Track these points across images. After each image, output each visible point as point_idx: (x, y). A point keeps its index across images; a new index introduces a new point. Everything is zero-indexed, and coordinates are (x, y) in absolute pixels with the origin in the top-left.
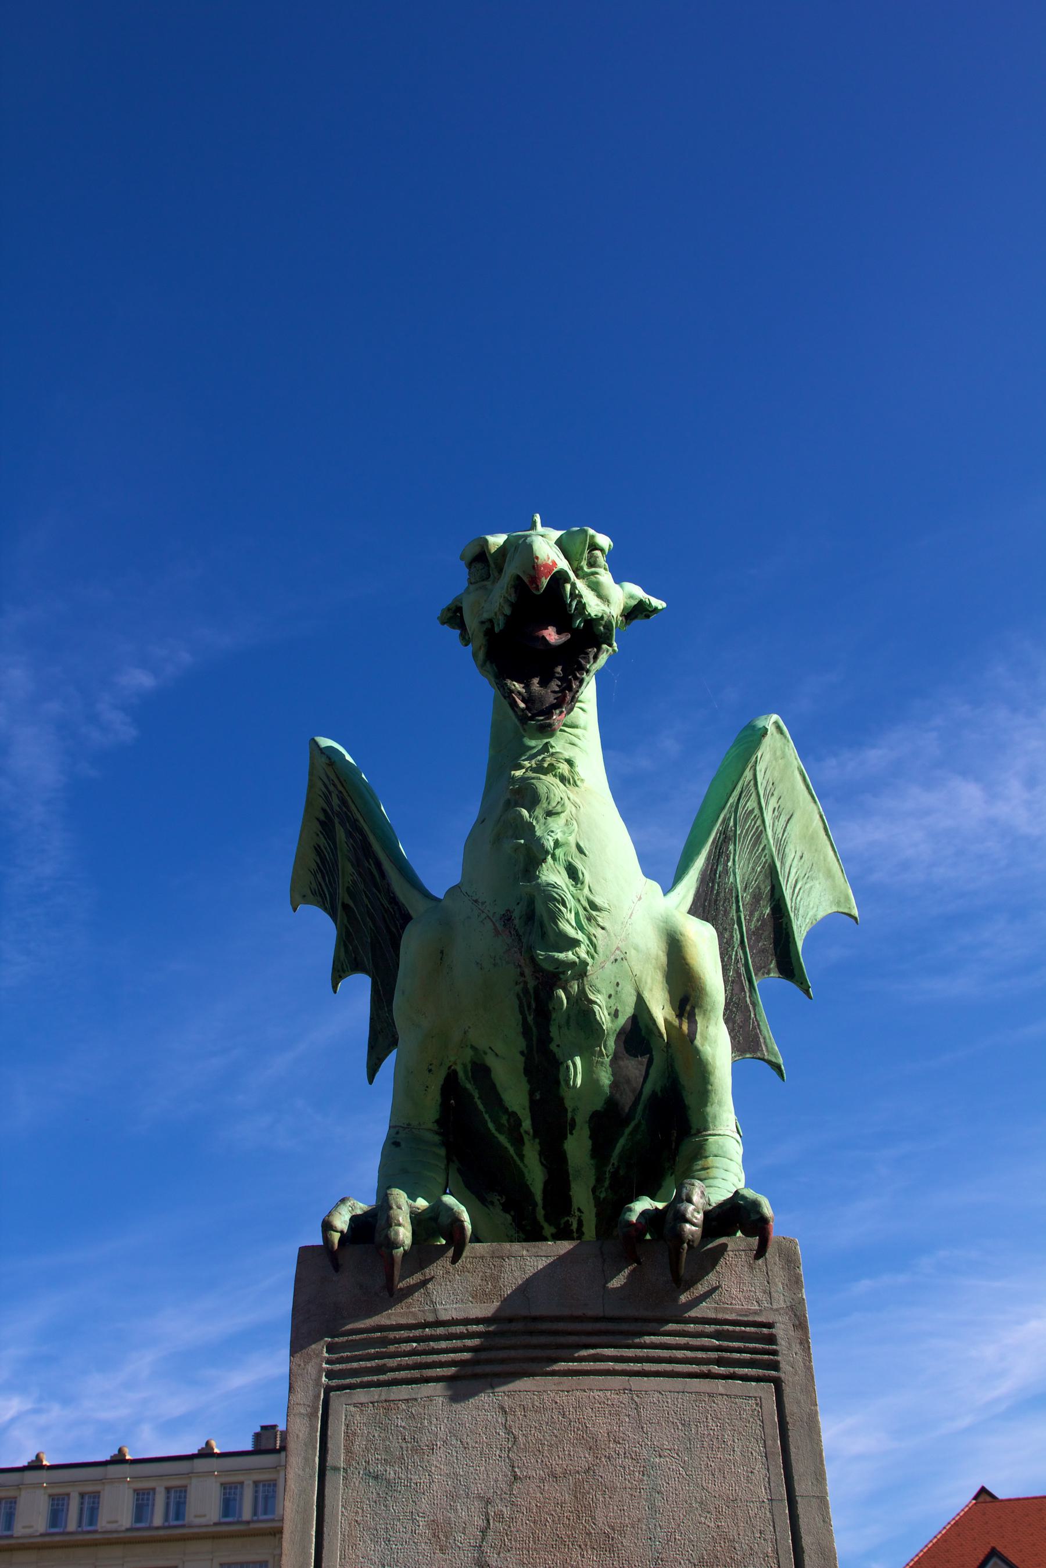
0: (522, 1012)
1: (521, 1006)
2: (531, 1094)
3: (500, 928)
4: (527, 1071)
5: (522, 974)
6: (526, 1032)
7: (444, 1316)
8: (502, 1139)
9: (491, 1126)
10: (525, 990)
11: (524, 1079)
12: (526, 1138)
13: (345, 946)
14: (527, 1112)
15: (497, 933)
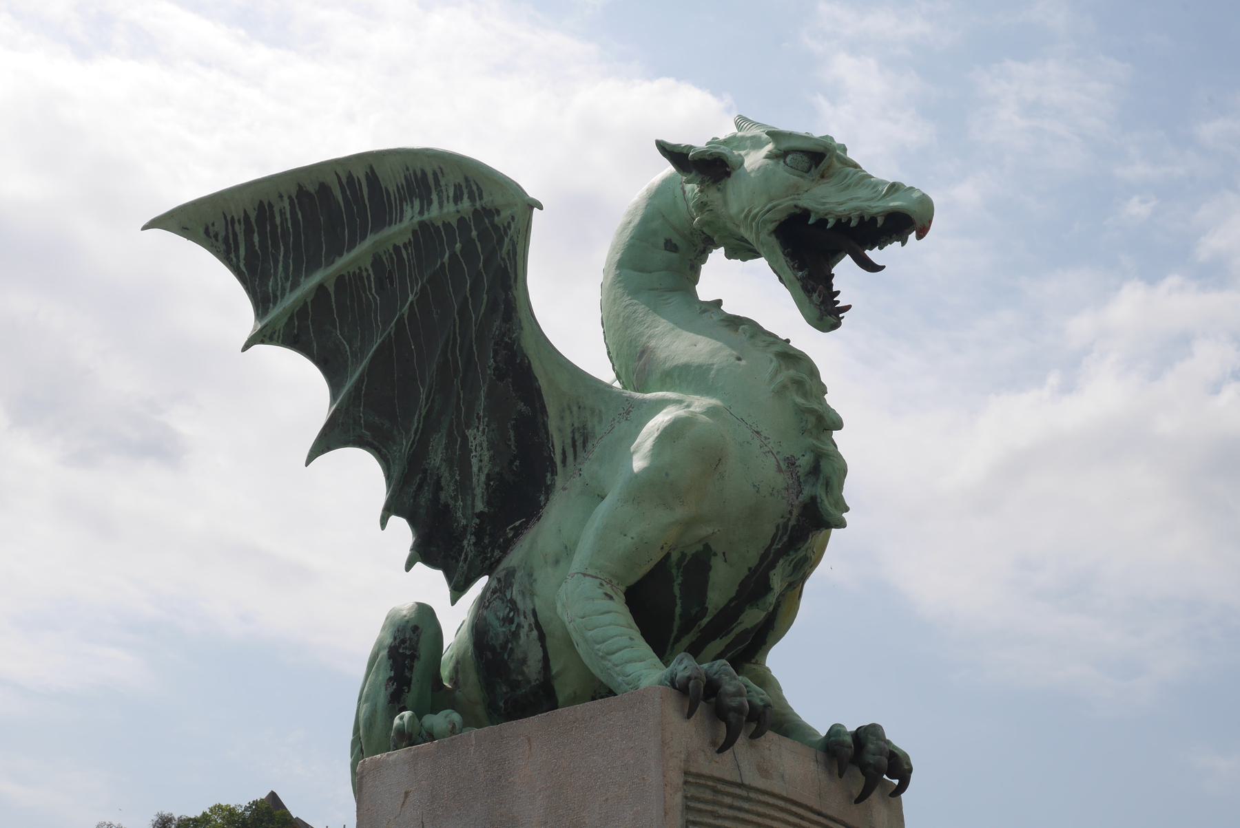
0: (773, 540)
1: (775, 535)
2: (731, 601)
3: (783, 466)
4: (743, 585)
5: (791, 513)
6: (763, 557)
7: (746, 782)
8: (677, 623)
9: (678, 610)
10: (785, 526)
11: (736, 588)
12: (696, 629)
13: (291, 319)
14: (715, 612)
15: (780, 470)
